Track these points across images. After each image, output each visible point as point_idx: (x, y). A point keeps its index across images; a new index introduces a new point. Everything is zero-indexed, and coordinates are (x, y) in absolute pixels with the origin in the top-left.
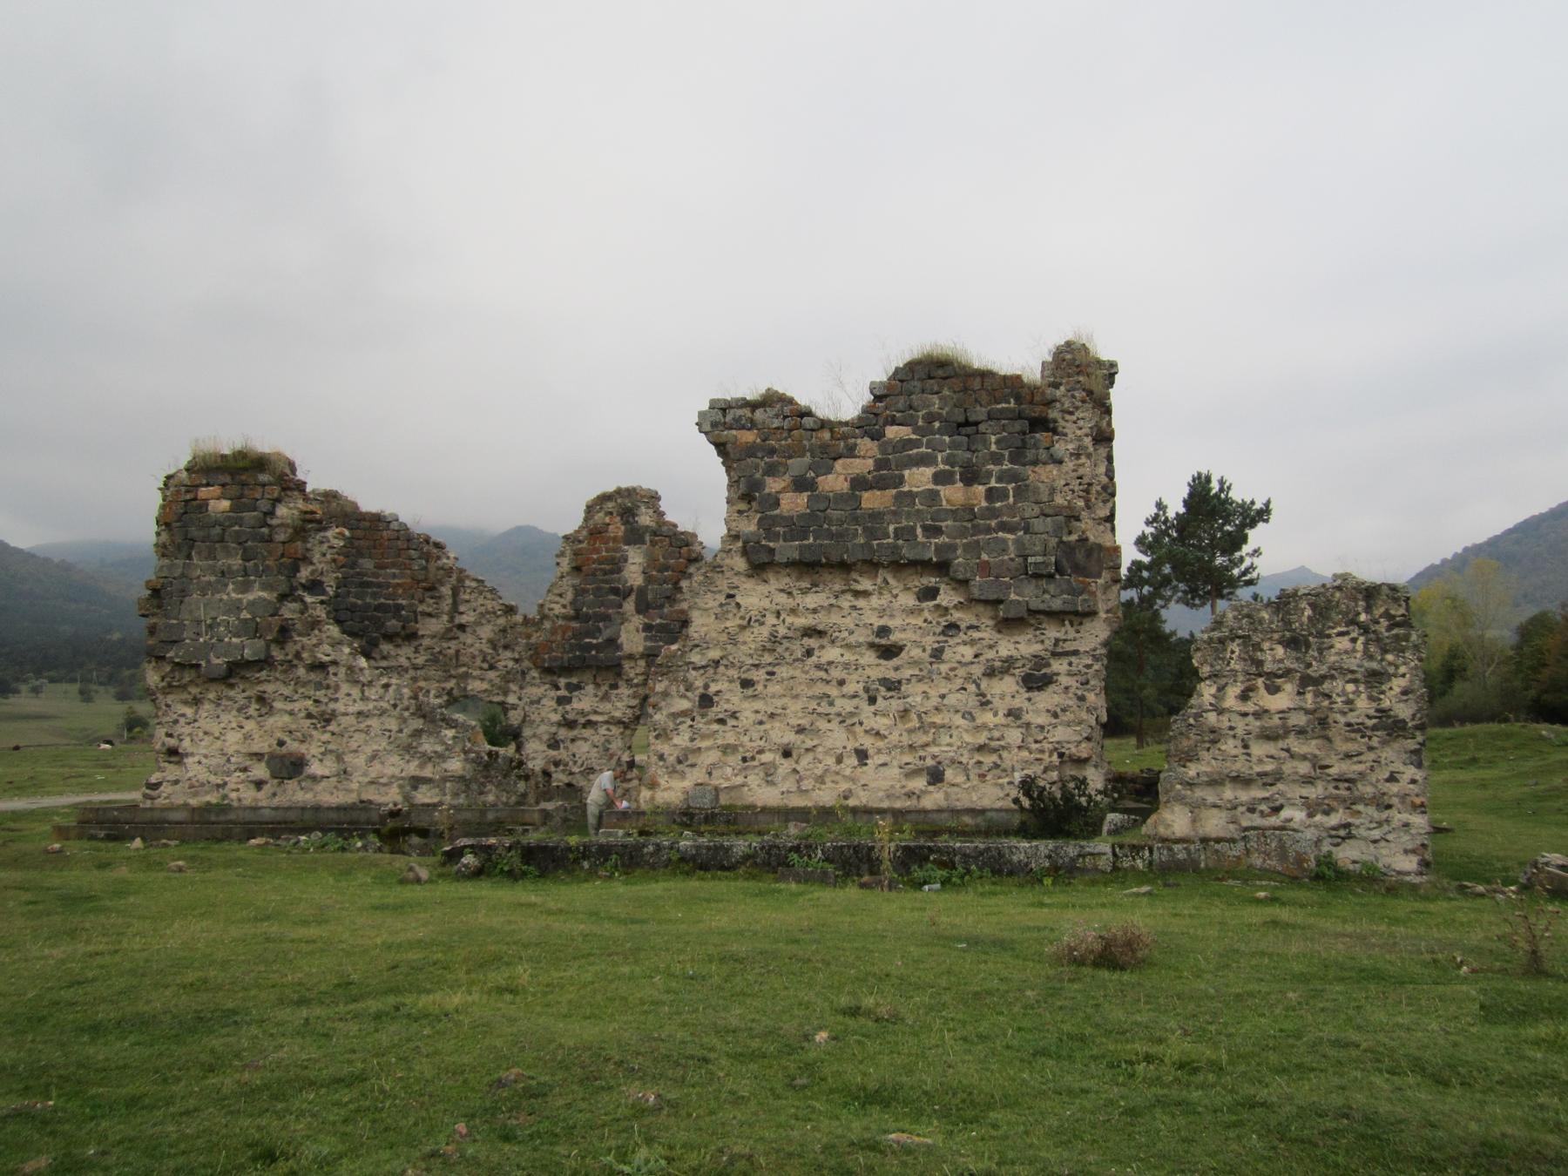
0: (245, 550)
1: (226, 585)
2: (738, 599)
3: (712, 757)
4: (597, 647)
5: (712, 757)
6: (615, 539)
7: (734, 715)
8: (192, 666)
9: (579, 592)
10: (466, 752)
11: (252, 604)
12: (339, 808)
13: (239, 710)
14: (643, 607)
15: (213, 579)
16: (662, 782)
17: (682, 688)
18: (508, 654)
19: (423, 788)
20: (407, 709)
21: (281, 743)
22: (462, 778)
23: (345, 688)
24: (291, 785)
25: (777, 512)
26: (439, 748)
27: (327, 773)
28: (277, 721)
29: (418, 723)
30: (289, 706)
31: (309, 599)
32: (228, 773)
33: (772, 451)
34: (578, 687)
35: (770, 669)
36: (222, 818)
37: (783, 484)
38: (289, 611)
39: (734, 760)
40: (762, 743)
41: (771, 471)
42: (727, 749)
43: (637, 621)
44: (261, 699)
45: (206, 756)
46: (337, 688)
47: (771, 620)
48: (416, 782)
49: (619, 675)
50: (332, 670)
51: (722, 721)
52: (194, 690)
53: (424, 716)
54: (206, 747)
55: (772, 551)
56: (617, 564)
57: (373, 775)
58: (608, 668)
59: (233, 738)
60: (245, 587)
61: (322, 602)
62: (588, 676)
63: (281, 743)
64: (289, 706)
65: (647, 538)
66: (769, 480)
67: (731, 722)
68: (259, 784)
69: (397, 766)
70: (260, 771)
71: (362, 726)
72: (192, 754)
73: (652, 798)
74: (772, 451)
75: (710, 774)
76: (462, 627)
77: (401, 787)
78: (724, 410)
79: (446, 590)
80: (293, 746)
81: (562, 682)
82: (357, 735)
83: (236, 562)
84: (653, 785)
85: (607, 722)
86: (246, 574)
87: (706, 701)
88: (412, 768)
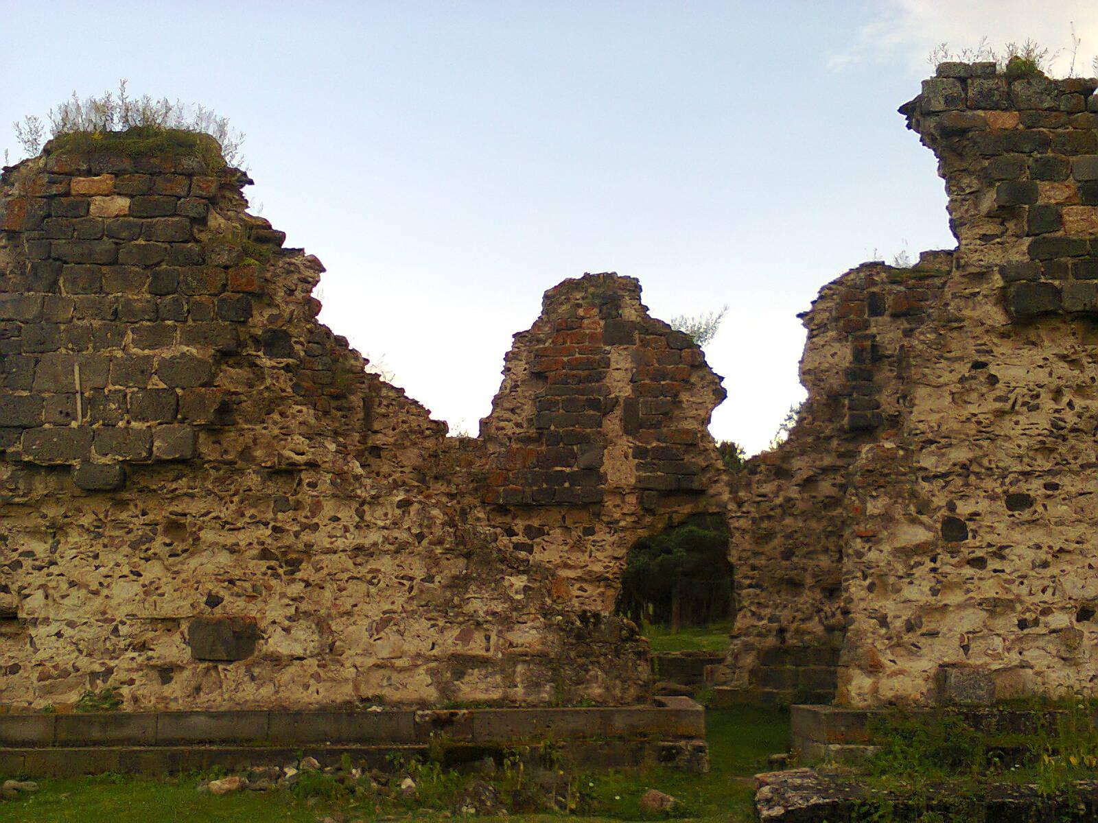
0: (156, 276)
1: (122, 335)
2: (993, 370)
3: (972, 619)
4: (569, 477)
5: (972, 619)
6: (592, 337)
7: (999, 553)
8: (52, 469)
9: (543, 405)
10: (546, 613)
11: (171, 363)
12: (323, 711)
13: (134, 546)
14: (632, 426)
15: (97, 323)
16: (884, 660)
17: (912, 509)
18: (444, 489)
19: (475, 674)
20: (440, 542)
21: (214, 601)
22: (541, 658)
23: (329, 508)
24: (233, 673)
25: (1060, 233)
26: (499, 607)
27: (298, 650)
28: (208, 563)
29: (457, 566)
30: (230, 539)
31: (266, 362)
32: (114, 654)
33: (1045, 143)
34: (540, 532)
35: (1049, 479)
36: (113, 733)
37: (1067, 193)
38: (231, 378)
39: (1007, 624)
40: (1047, 596)
41: (1047, 172)
42: (994, 607)
43: (625, 443)
44: (174, 526)
45: (71, 624)
46: (316, 508)
47: (1047, 403)
48: (461, 664)
49: (598, 515)
50: (306, 477)
51: (979, 563)
52: (53, 511)
53: (468, 556)
54: (74, 608)
55: (1057, 292)
56: (597, 369)
57: (385, 654)
58: (585, 506)
59: (124, 593)
60: (158, 338)
61: (287, 368)
62: (554, 516)
63: (214, 601)
64: (230, 539)
65: (636, 335)
66: (1044, 186)
67: (993, 564)
68: (166, 672)
69: (423, 637)
70: (172, 648)
71: (363, 570)
72: (46, 621)
73: (875, 690)
74: (1045, 143)
75: (966, 648)
76: (376, 451)
77: (432, 672)
78: (963, 80)
79: (356, 400)
80: (234, 605)
81: (519, 525)
82: (351, 586)
83: (141, 297)
84: (874, 668)
85: (580, 579)
86: (157, 315)
87: (954, 529)
88: (449, 641)
